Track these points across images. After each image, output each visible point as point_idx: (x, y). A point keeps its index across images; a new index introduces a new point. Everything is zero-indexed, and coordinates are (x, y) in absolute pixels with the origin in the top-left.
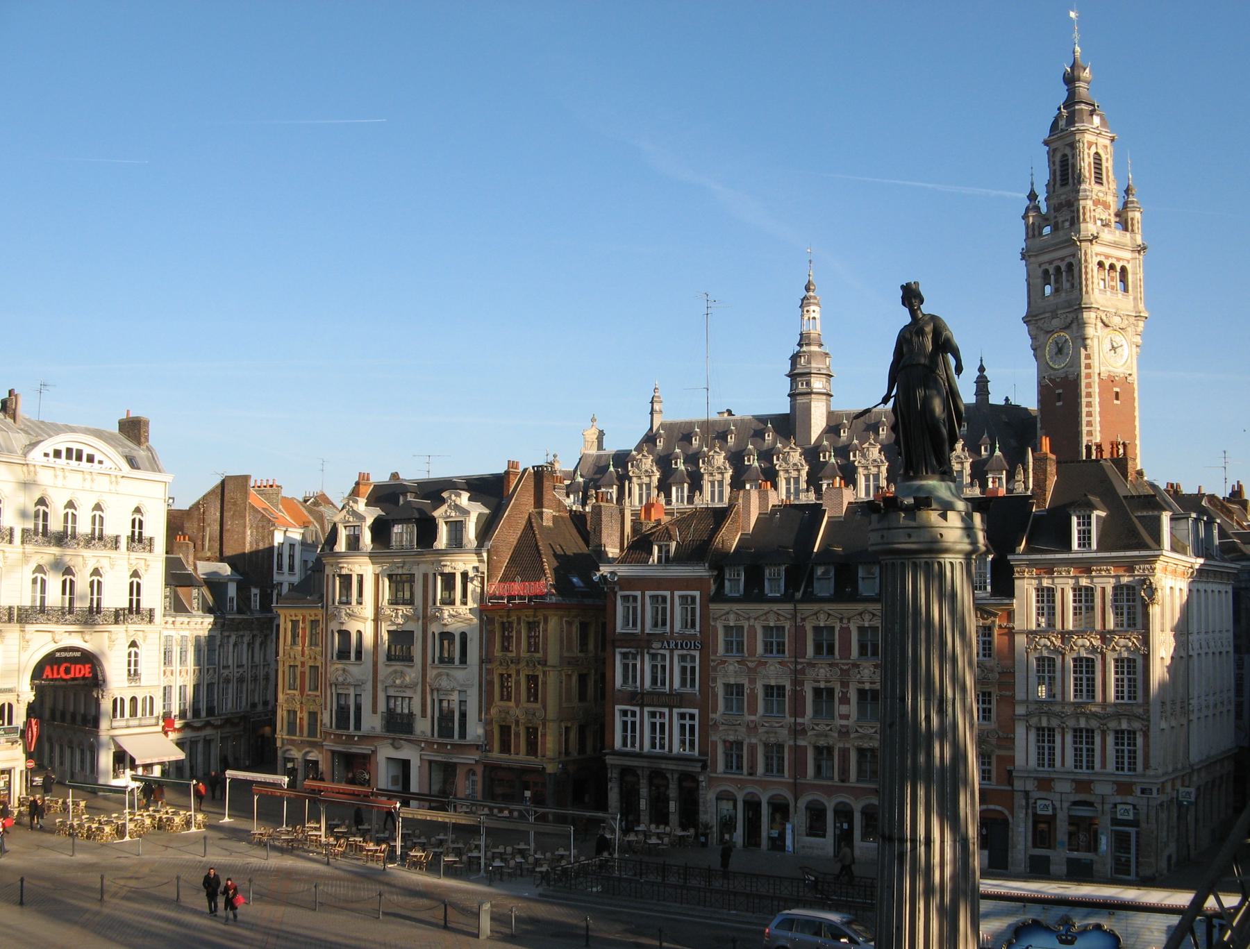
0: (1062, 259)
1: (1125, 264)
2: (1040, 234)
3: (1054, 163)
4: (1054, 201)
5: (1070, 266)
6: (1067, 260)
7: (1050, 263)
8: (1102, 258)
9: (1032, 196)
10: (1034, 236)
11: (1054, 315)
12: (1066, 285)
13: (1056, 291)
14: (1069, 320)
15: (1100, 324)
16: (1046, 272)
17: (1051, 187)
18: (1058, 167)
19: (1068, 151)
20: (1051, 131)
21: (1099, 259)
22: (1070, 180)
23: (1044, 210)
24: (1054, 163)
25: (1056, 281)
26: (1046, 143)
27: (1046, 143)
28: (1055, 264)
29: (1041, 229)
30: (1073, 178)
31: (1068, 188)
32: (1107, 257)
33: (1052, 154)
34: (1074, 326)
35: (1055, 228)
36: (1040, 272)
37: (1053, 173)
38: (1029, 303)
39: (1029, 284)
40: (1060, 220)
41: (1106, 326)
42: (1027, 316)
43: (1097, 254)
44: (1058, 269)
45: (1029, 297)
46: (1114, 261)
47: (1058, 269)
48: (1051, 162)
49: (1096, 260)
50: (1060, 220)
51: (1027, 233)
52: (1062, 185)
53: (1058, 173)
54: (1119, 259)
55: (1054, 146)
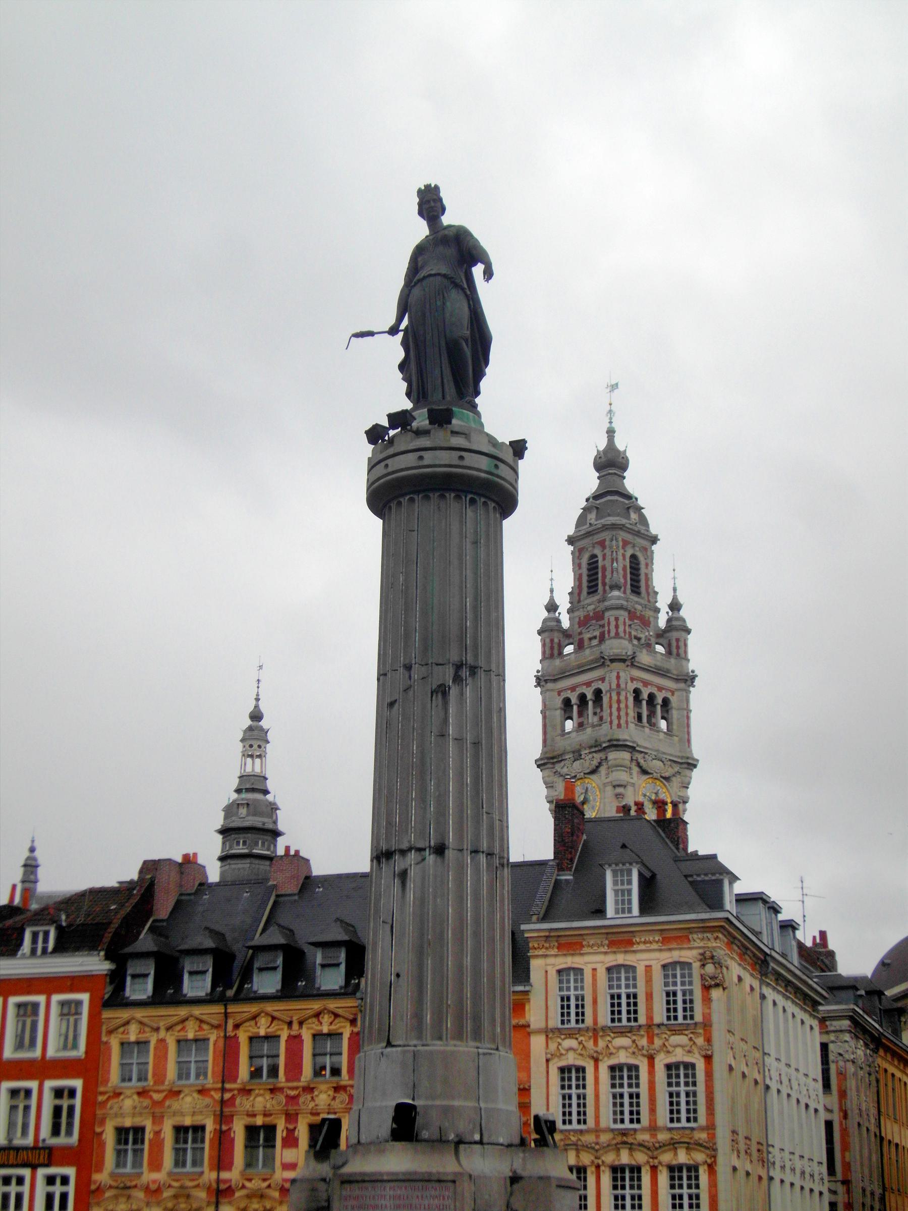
0: (588, 684)
1: (669, 695)
2: (560, 653)
3: (580, 566)
4: (581, 613)
5: (598, 693)
6: (595, 686)
7: (573, 689)
8: (639, 685)
9: (552, 607)
10: (552, 656)
11: (577, 755)
12: (592, 719)
13: (581, 725)
14: (595, 763)
15: (636, 769)
16: (567, 703)
17: (575, 596)
18: (584, 571)
19: (597, 551)
20: (577, 526)
21: (636, 685)
22: (600, 587)
23: (566, 623)
24: (580, 566)
25: (580, 714)
26: (571, 541)
27: (571, 541)
28: (579, 691)
29: (561, 648)
30: (604, 584)
31: (596, 598)
32: (646, 684)
33: (577, 556)
34: (603, 770)
35: (580, 646)
36: (558, 702)
37: (578, 579)
38: (545, 741)
39: (544, 718)
40: (586, 636)
41: (644, 772)
42: (541, 759)
43: (632, 679)
44: (583, 698)
45: (545, 733)
46: (654, 690)
47: (583, 698)
48: (577, 565)
49: (632, 686)
50: (586, 636)
51: (544, 653)
52: (589, 593)
53: (585, 579)
54: (660, 689)
55: (581, 544)
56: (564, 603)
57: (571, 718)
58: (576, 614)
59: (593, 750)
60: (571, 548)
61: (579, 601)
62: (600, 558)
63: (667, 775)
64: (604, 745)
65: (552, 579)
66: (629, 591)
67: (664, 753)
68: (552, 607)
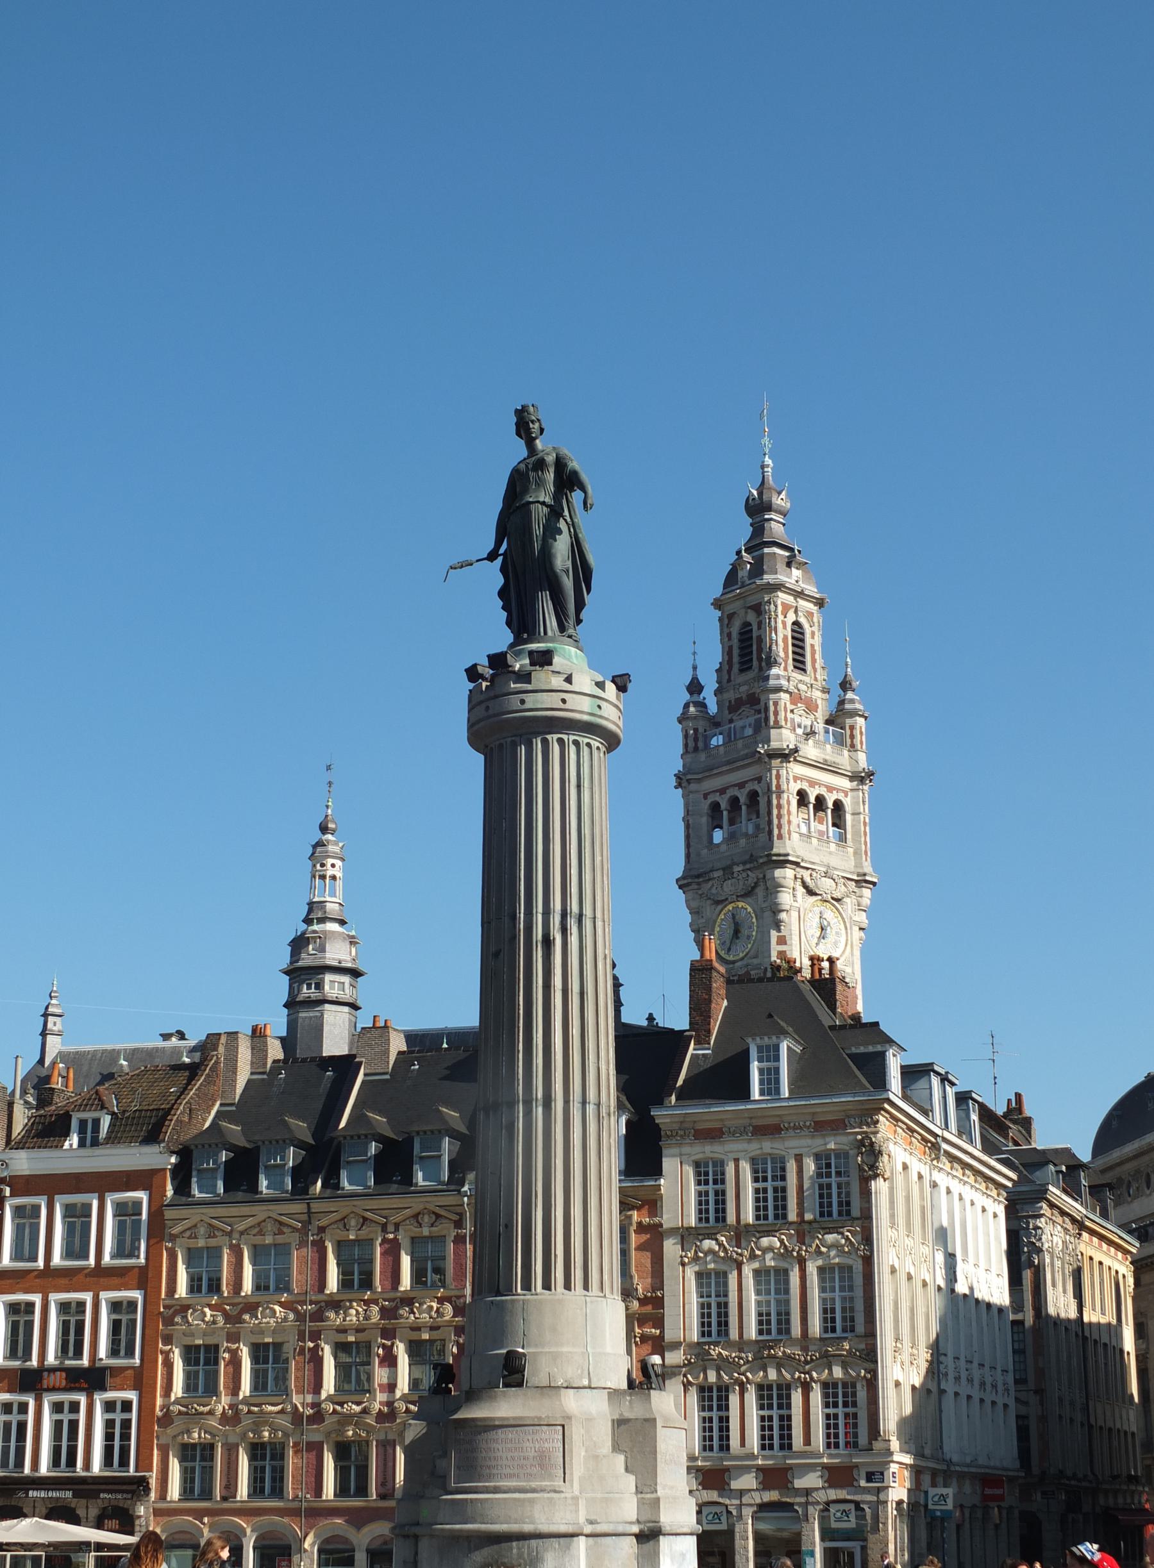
0: (741, 785)
4: (730, 695)
7: (722, 791)
8: (805, 786)
9: (695, 687)
15: (801, 890)
16: (715, 807)
18: (735, 642)
23: (713, 708)
25: (732, 822)
32: (812, 783)
33: (726, 621)
44: (734, 802)
46: (823, 791)
47: (734, 802)
49: (795, 787)
52: (741, 671)
53: (736, 652)
54: (830, 789)
56: (710, 684)
57: (721, 827)
58: (726, 696)
59: (748, 866)
60: (719, 613)
61: (729, 680)
62: (755, 627)
63: (837, 895)
64: (761, 861)
65: (694, 653)
66: (790, 667)
67: (836, 869)
68: (695, 687)
